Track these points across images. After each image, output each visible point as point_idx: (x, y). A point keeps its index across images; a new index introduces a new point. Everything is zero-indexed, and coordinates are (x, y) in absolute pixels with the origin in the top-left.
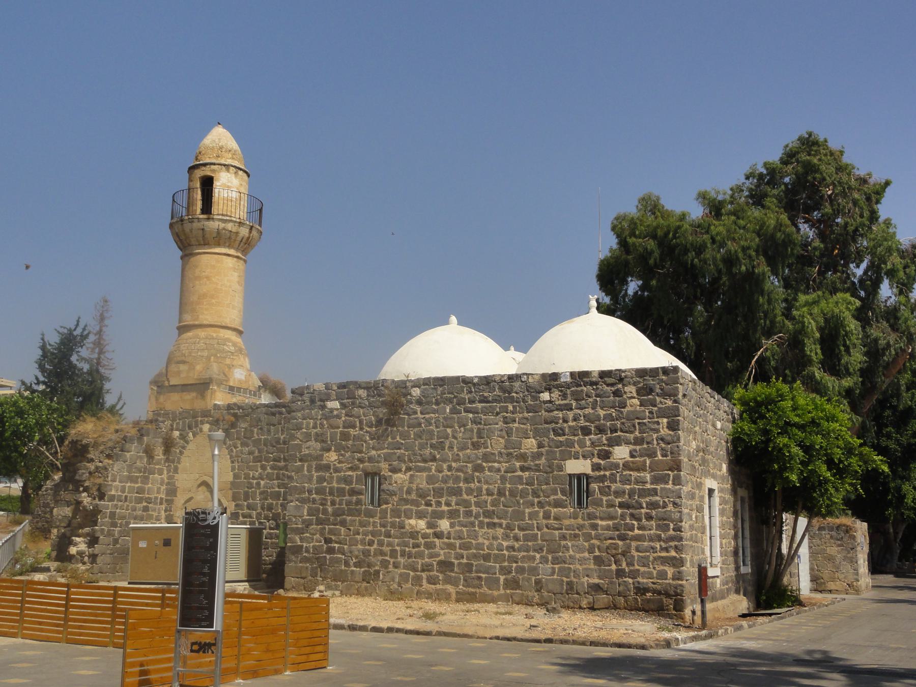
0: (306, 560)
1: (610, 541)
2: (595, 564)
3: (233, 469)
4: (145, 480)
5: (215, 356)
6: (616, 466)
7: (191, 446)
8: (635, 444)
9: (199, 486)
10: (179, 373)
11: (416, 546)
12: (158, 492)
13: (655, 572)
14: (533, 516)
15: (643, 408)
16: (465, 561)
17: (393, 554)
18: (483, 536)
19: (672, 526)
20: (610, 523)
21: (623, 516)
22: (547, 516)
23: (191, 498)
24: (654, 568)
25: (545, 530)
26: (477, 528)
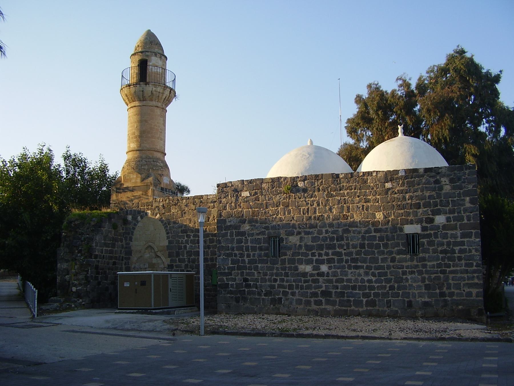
0: (231, 292)
1: (435, 275)
2: (425, 290)
3: (168, 238)
4: (113, 246)
5: (152, 169)
6: (438, 227)
7: (140, 224)
8: (450, 213)
9: (147, 248)
11: (305, 282)
12: (121, 253)
13: (464, 293)
14: (383, 260)
15: (454, 191)
16: (339, 290)
17: (291, 287)
18: (351, 274)
19: (475, 264)
20: (435, 263)
21: (443, 259)
22: (393, 260)
23: (141, 256)
24: (464, 291)
25: (392, 269)
26: (347, 269)
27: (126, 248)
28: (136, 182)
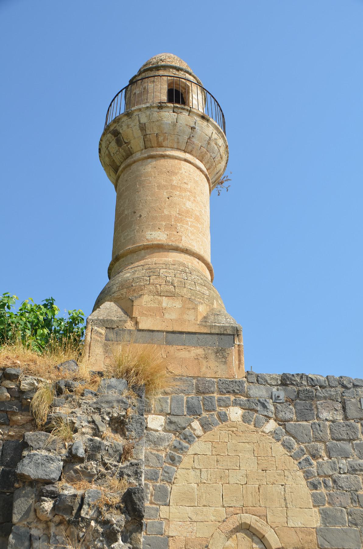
3: (317, 501)
7: (197, 447)
10: (162, 311)
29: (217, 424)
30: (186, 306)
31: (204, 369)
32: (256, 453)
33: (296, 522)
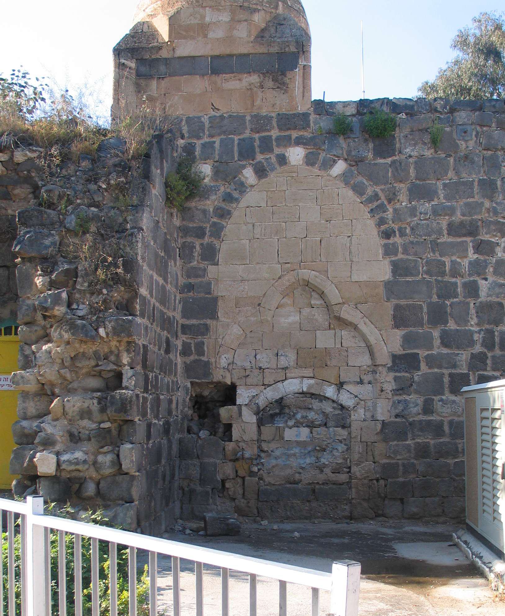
3: (389, 251)
9: (289, 292)
27: (190, 287)
28: (229, 39)
29: (273, 169)
30: (237, 18)
31: (258, 103)
32: (319, 200)
33: (361, 275)
